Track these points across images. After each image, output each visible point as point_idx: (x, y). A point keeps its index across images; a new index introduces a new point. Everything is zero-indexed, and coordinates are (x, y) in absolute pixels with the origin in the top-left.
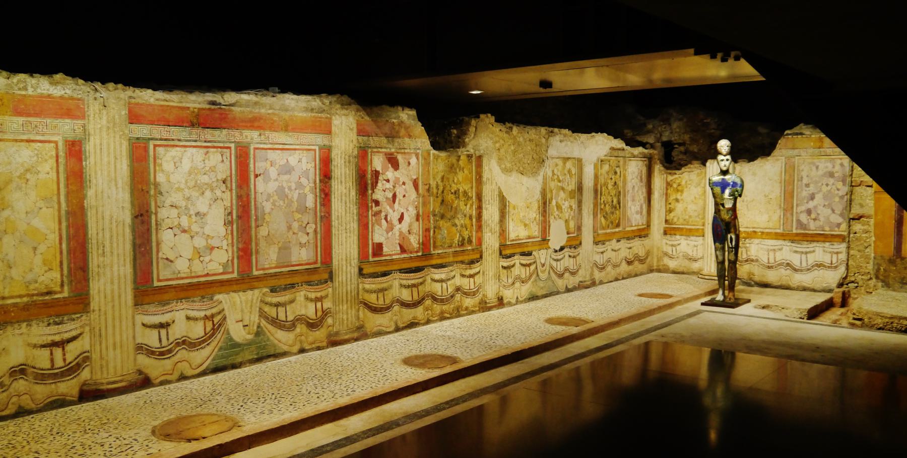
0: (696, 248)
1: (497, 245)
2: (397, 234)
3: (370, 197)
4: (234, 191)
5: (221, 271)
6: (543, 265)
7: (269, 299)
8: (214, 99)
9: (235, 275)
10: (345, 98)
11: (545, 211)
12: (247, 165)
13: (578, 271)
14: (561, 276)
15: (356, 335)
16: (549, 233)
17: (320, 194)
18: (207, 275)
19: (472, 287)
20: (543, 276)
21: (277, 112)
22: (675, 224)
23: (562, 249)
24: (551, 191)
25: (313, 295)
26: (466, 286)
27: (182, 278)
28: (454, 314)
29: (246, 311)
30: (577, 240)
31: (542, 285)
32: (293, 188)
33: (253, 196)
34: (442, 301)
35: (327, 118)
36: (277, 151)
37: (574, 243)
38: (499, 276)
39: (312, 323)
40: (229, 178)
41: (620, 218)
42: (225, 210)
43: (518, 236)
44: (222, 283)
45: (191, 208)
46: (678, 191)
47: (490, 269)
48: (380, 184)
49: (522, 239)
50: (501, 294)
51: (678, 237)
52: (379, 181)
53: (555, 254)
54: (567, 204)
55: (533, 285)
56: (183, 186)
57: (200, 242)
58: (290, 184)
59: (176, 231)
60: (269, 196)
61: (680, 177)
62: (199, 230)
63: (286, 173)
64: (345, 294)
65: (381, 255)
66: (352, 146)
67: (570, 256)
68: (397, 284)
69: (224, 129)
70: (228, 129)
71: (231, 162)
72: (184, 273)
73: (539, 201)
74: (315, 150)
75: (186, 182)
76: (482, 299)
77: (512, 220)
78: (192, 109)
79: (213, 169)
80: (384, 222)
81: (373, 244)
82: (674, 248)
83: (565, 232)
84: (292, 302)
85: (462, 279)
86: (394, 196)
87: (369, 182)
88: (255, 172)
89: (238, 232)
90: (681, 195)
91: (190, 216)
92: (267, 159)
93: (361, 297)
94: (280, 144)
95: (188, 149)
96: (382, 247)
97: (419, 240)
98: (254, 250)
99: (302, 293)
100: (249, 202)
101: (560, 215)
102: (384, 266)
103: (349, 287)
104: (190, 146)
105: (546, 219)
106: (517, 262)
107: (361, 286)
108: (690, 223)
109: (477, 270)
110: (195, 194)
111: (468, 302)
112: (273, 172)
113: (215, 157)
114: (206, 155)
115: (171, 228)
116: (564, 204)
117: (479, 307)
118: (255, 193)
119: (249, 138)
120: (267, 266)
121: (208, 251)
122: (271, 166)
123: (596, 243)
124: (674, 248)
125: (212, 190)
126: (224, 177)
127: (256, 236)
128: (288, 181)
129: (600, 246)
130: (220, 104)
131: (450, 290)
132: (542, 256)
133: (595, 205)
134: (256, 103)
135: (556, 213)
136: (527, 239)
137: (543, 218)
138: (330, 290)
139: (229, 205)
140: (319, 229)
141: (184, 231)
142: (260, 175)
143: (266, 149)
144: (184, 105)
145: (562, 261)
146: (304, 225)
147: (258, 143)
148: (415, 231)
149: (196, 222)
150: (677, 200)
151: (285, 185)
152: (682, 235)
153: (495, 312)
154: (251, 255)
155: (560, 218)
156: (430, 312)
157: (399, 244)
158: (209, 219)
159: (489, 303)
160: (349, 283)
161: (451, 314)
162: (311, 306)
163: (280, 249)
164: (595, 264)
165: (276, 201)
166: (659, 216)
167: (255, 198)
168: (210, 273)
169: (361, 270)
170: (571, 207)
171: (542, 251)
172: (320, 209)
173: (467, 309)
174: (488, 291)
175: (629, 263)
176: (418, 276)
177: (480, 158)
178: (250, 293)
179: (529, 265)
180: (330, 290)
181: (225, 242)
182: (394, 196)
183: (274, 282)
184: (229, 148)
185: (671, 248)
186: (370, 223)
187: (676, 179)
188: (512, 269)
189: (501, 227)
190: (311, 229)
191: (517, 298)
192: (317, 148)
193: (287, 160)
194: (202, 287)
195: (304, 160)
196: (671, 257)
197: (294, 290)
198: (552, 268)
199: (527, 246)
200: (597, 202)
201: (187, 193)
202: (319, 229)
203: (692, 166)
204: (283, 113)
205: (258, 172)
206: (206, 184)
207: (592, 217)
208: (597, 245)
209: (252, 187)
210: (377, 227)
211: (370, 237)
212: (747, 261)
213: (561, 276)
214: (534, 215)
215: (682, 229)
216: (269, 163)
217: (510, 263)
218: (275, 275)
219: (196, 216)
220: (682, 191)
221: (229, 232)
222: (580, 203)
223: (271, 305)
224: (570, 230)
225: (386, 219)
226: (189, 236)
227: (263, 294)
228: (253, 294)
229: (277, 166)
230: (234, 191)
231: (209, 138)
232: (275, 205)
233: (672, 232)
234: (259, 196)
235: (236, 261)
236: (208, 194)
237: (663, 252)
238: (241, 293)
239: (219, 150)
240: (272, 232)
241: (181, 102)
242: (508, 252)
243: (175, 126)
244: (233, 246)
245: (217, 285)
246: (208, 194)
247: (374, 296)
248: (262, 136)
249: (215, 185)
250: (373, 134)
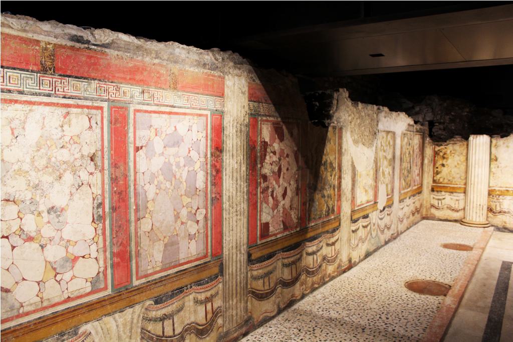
0: (457, 202)
2: (281, 210)
3: (259, 172)
4: (106, 172)
5: (89, 290)
6: (374, 225)
7: (153, 314)
8: (80, 34)
9: (109, 291)
10: (236, 56)
12: (125, 134)
15: (244, 330)
17: (212, 171)
18: (69, 299)
20: (374, 234)
21: (165, 63)
22: (441, 183)
25: (202, 297)
27: (27, 314)
29: (124, 336)
32: (182, 164)
33: (132, 178)
35: (220, 77)
36: (164, 116)
37: (389, 205)
39: (202, 330)
40: (100, 153)
42: (94, 199)
44: (90, 307)
45: (41, 202)
48: (268, 157)
51: (443, 193)
52: (268, 154)
54: (387, 170)
56: (26, 167)
57: (55, 253)
58: (178, 160)
59: (15, 240)
60: (154, 177)
61: (446, 148)
62: (52, 233)
63: (173, 145)
64: (234, 286)
65: (268, 236)
66: (243, 113)
68: (280, 265)
69: (94, 79)
70: (100, 80)
71: (102, 128)
72: (31, 304)
74: (207, 116)
75: (33, 159)
78: (43, 44)
79: (75, 140)
80: (270, 198)
81: (261, 224)
84: (180, 310)
86: (280, 170)
87: (259, 154)
88: (135, 144)
89: (112, 229)
90: (446, 162)
91: (39, 214)
92: (151, 126)
93: (249, 287)
94: (167, 106)
95: (35, 107)
96: (269, 227)
97: (298, 214)
98: (133, 253)
99: (191, 297)
100: (126, 186)
102: (270, 247)
103: (238, 277)
104: (40, 104)
107: (249, 275)
108: (453, 182)
110: (47, 179)
111: (331, 269)
112: (158, 144)
113: (79, 121)
114: (65, 117)
115: (7, 237)
118: (136, 173)
119: (129, 95)
120: (150, 272)
121: (69, 264)
122: (156, 135)
124: (440, 202)
125: (74, 172)
126: (93, 151)
127: (136, 233)
128: (176, 155)
130: (88, 42)
132: (374, 216)
134: (139, 48)
135: (382, 178)
138: (220, 285)
139: (100, 192)
140: (209, 215)
141: (30, 239)
142: (142, 147)
143: (150, 112)
144: (30, 35)
146: (194, 211)
147: (139, 103)
148: (295, 206)
149: (49, 222)
150: (443, 165)
151: (172, 161)
154: (130, 259)
156: (304, 287)
157: (283, 221)
158: (69, 215)
160: (239, 273)
162: (201, 310)
163: (166, 245)
165: (162, 183)
167: (135, 180)
168: (72, 296)
169: (249, 255)
172: (211, 190)
176: (297, 253)
177: (341, 129)
178: (129, 311)
180: (220, 285)
181: (94, 247)
182: (280, 170)
183: (158, 291)
184: (101, 108)
185: (437, 201)
186: (259, 201)
188: (358, 232)
190: (200, 217)
192: (208, 113)
193: (175, 127)
194: (59, 319)
195: (195, 128)
197: (182, 295)
201: (34, 177)
202: (209, 215)
203: (455, 139)
204: (171, 66)
205: (138, 144)
206: (64, 162)
209: (131, 164)
210: (264, 205)
211: (259, 217)
212: (500, 212)
215: (447, 187)
216: (153, 131)
218: (161, 280)
219: (49, 213)
220: (447, 159)
221: (100, 232)
223: (155, 320)
225: (272, 195)
226: (38, 245)
227: (146, 309)
228: (134, 312)
229: (163, 135)
230: (106, 172)
231: (71, 92)
232: (160, 189)
233: (439, 189)
234: (140, 176)
235: (109, 271)
236: (68, 177)
237: (431, 204)
238: (117, 315)
239: (86, 110)
240: (157, 224)
241: (25, 31)
243: (14, 69)
244: (105, 251)
245: (84, 310)
246: (68, 177)
247: (261, 281)
248: (146, 95)
249: (78, 163)
250: (263, 101)
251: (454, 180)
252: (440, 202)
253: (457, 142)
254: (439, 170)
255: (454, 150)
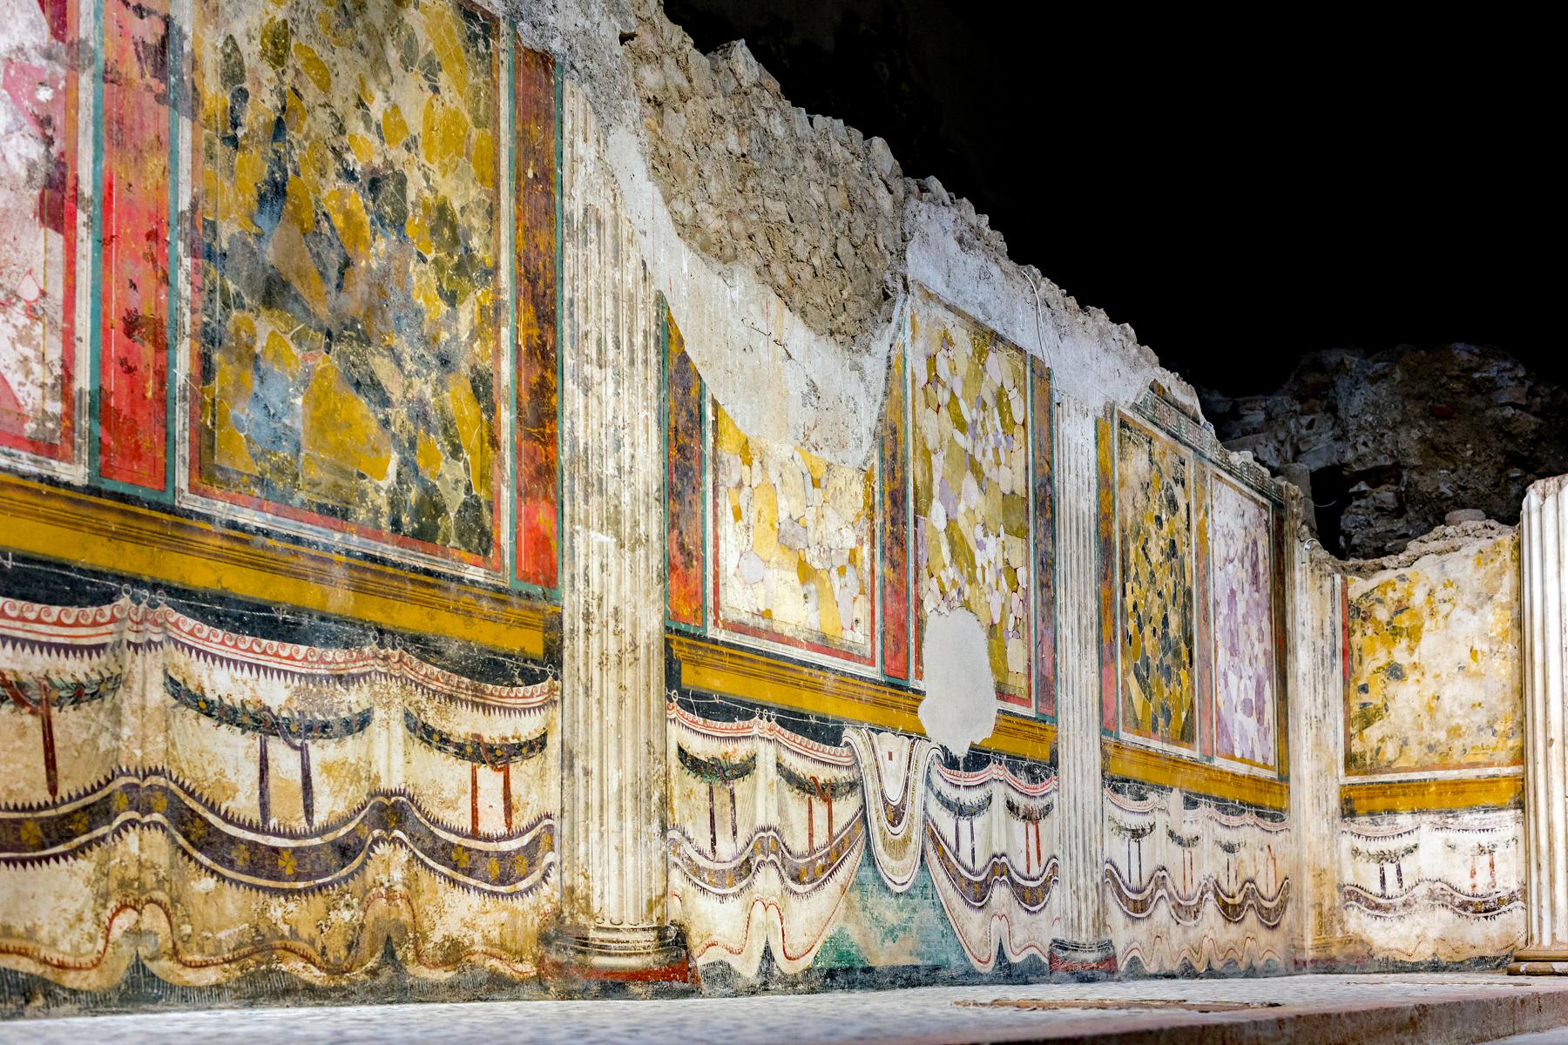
0: (1486, 858)
1: (651, 623)
6: (896, 816)
11: (899, 540)
13: (1045, 888)
14: (978, 894)
16: (919, 660)
19: (492, 822)
20: (899, 870)
22: (1389, 767)
23: (978, 759)
24: (927, 454)
26: (451, 805)
28: (359, 975)
30: (1041, 740)
31: (891, 917)
34: (263, 862)
38: (665, 802)
41: (1192, 705)
43: (767, 614)
46: (1396, 632)
47: (612, 749)
49: (790, 641)
50: (675, 911)
51: (1404, 820)
53: (948, 774)
55: (850, 906)
61: (1402, 578)
67: (1011, 807)
73: (869, 477)
76: (558, 915)
77: (738, 515)
82: (1390, 870)
83: (989, 682)
85: (419, 750)
90: (1411, 650)
101: (967, 590)
105: (902, 581)
106: (767, 756)
108: (1456, 756)
109: (528, 727)
116: (981, 546)
117: (540, 962)
123: (1115, 783)
129: (1127, 800)
131: (328, 805)
133: (1106, 607)
136: (811, 646)
137: (891, 575)
145: (978, 821)
150: (1395, 672)
152: (1421, 812)
153: (642, 1008)
155: (966, 605)
159: (603, 950)
161: (335, 970)
164: (1112, 876)
166: (1318, 744)
170: (1010, 571)
171: (887, 736)
173: (454, 953)
174: (596, 871)
175: (1231, 912)
179: (828, 792)
187: (1383, 586)
188: (740, 787)
189: (673, 522)
191: (768, 955)
196: (1378, 907)
198: (937, 844)
199: (815, 688)
200: (1112, 597)
203: (1450, 530)
207: (1093, 655)
208: (1116, 790)
213: (978, 894)
214: (849, 539)
215: (1423, 785)
217: (730, 747)
220: (1414, 634)
222: (1046, 565)
224: (1011, 681)
233: (1380, 803)
237: (1340, 887)
242: (717, 682)
251: (1458, 744)
252: (1390, 870)
253: (1457, 542)
254: (1373, 698)
255: (1448, 584)
